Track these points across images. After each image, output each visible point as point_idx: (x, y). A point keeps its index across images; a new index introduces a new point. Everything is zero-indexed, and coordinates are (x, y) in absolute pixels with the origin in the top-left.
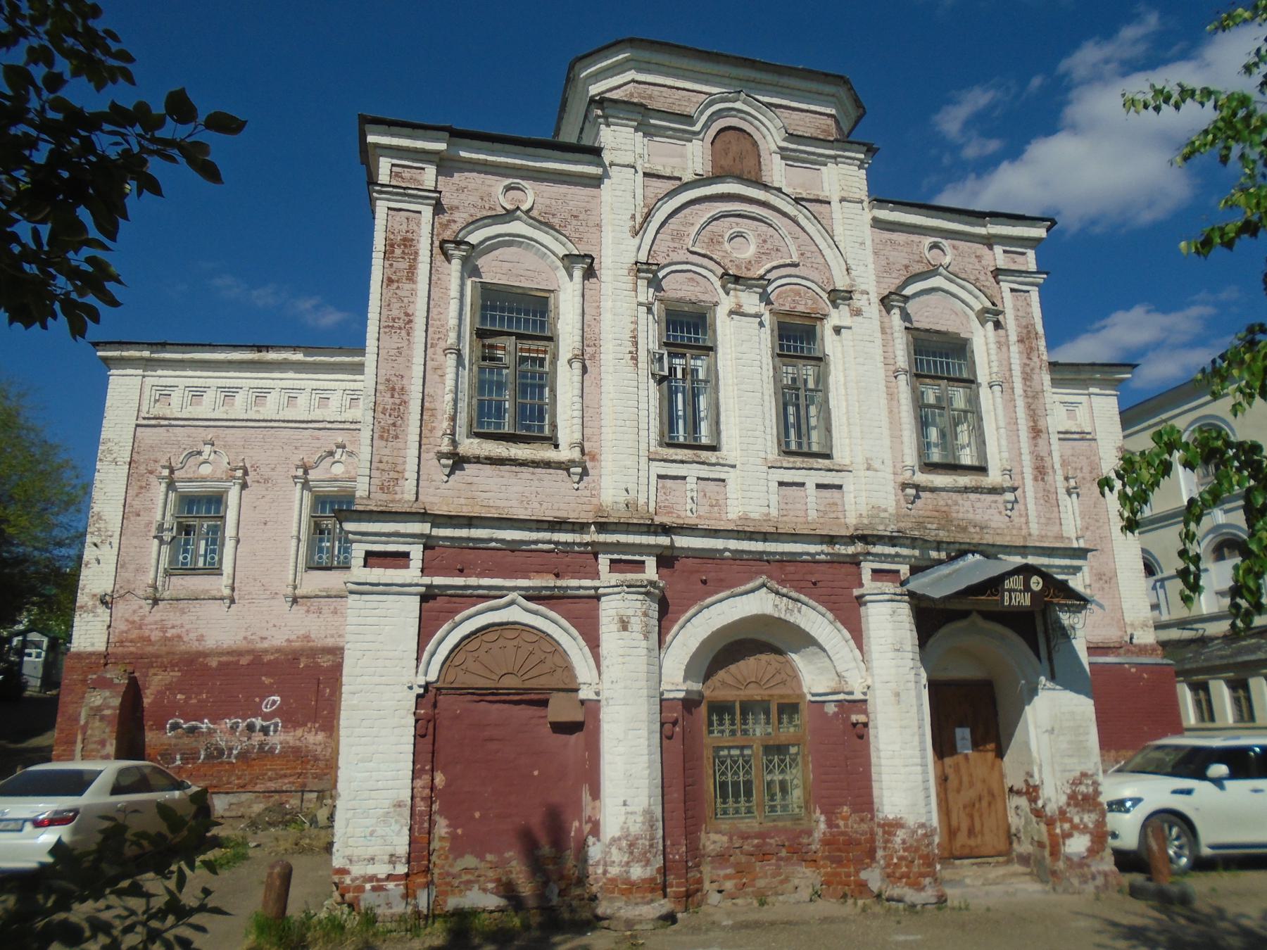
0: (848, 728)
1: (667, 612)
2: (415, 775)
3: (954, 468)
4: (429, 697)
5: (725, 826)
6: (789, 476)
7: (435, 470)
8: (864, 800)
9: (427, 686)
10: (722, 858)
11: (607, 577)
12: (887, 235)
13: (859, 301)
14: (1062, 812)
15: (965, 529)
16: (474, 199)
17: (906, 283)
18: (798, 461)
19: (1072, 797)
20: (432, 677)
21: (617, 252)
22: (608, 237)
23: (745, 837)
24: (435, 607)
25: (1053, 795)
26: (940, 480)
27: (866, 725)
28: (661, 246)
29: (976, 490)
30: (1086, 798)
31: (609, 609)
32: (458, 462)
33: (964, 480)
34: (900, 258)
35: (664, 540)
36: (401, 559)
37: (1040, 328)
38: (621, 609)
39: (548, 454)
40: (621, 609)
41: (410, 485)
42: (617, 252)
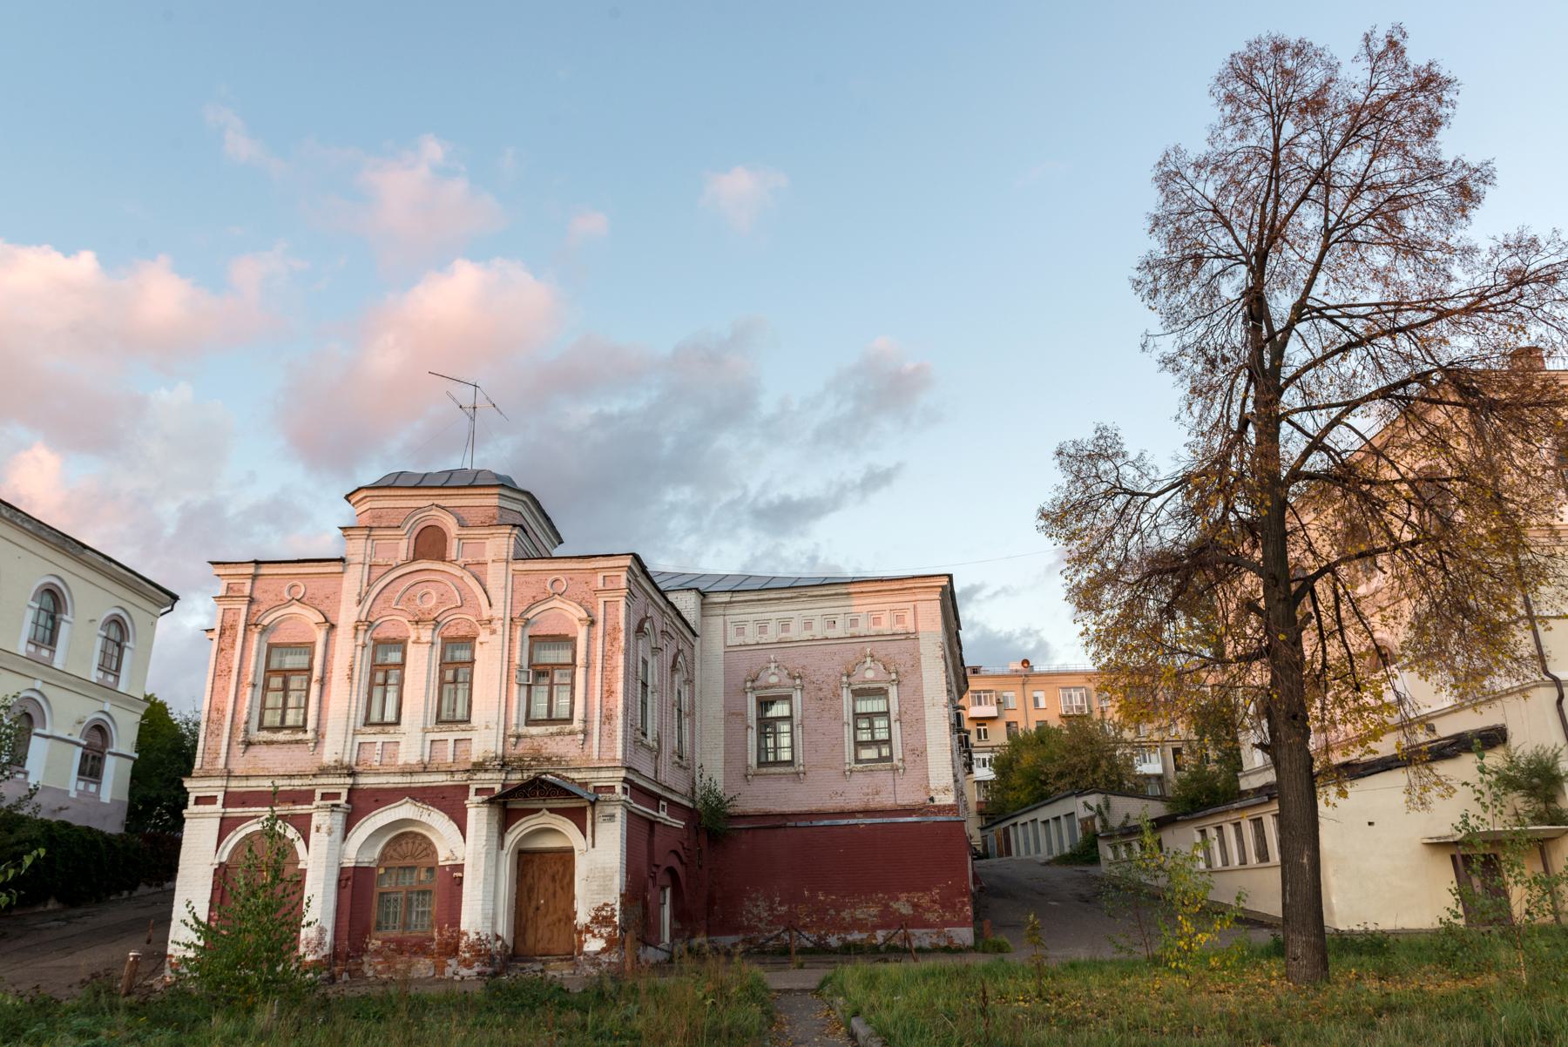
0: (453, 879)
1: (350, 823)
2: (210, 910)
3: (550, 721)
4: (222, 873)
5: (379, 934)
6: (437, 736)
7: (238, 749)
8: (455, 920)
9: (221, 864)
10: (377, 952)
11: (318, 801)
12: (523, 579)
13: (497, 625)
14: (587, 927)
15: (549, 759)
16: (272, 596)
17: (529, 609)
18: (445, 727)
19: (595, 919)
20: (224, 859)
21: (347, 615)
22: (343, 608)
23: (390, 941)
24: (226, 826)
25: (583, 917)
26: (534, 730)
27: (461, 878)
28: (376, 609)
29: (558, 734)
30: (605, 918)
31: (316, 820)
32: (248, 744)
33: (554, 729)
34: (529, 593)
35: (349, 781)
36: (211, 800)
37: (622, 626)
38: (323, 820)
39: (300, 736)
40: (323, 820)
41: (222, 761)
42: (347, 615)
